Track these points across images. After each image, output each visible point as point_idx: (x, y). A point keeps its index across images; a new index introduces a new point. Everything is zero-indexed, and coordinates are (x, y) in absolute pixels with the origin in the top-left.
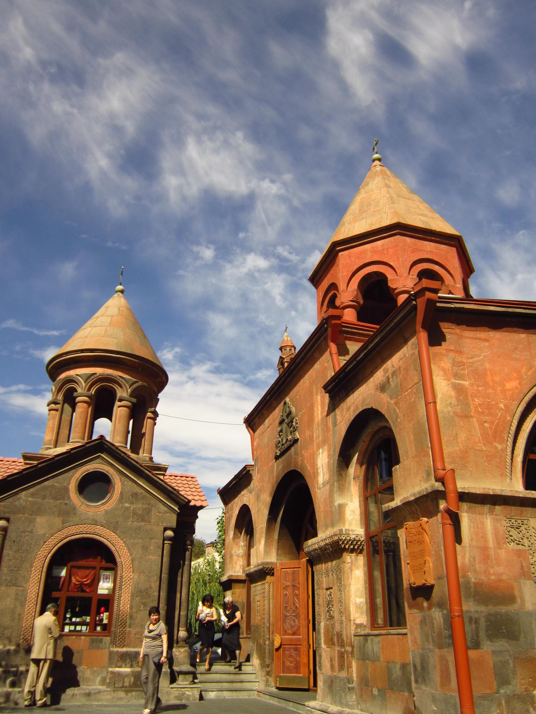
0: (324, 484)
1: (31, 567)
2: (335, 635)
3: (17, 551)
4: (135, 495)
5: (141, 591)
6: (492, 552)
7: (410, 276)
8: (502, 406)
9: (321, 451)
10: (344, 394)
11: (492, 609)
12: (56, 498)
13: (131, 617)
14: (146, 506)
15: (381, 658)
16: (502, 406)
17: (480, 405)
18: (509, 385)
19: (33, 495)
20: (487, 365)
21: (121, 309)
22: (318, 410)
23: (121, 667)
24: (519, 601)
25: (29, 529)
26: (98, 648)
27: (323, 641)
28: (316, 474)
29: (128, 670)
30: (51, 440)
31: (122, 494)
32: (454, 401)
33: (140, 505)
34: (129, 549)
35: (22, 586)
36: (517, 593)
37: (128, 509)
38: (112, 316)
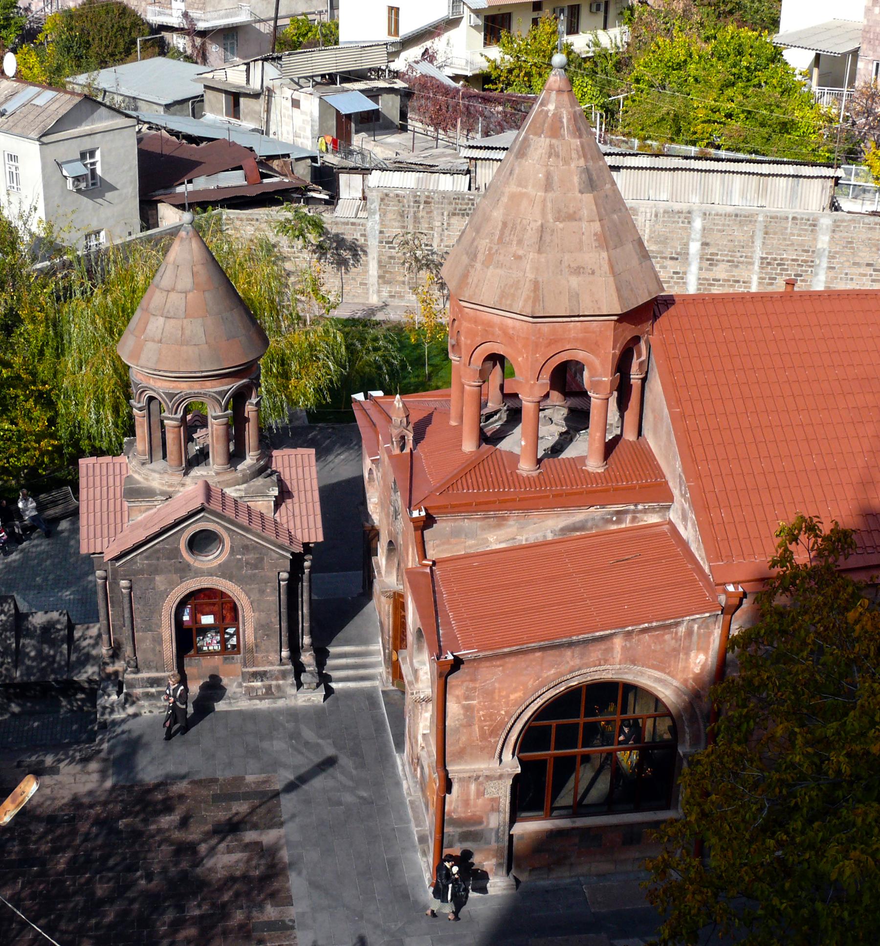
1: (161, 616)
5: (263, 626)
6: (472, 802)
7: (540, 381)
8: (503, 712)
11: (465, 829)
12: (169, 559)
13: (257, 646)
16: (503, 712)
17: (483, 715)
18: (512, 697)
19: (147, 558)
20: (497, 685)
21: (195, 269)
24: (485, 824)
25: (151, 587)
26: (232, 663)
29: (259, 684)
30: (144, 451)
31: (232, 547)
32: (462, 717)
34: (247, 595)
36: (484, 820)
37: (239, 559)
38: (186, 292)
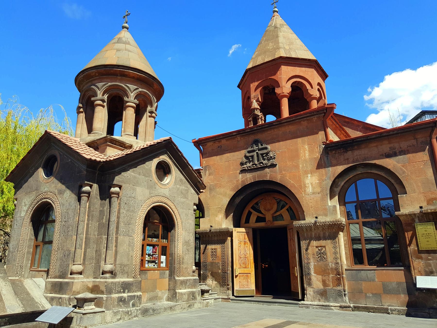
0: (313, 193)
2: (329, 269)
3: (128, 210)
4: (181, 180)
5: (186, 242)
9: (309, 175)
10: (342, 151)
14: (186, 188)
15: (376, 280)
22: (305, 153)
23: (181, 289)
27: (312, 272)
28: (303, 187)
33: (184, 188)
35: (132, 236)
37: (178, 189)
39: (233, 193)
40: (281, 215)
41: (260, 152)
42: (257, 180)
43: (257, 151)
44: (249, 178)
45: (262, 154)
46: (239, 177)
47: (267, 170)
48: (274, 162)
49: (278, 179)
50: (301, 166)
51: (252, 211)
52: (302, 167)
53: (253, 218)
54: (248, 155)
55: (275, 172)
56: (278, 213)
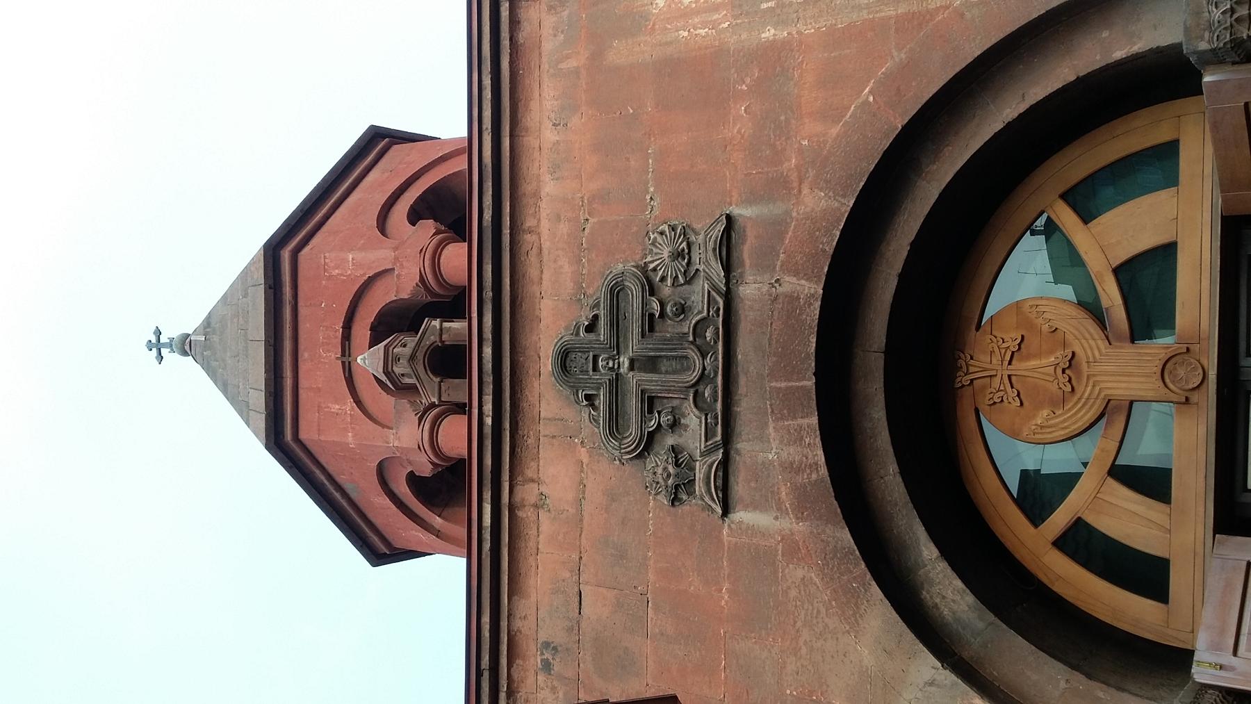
39: (878, 613)
40: (1126, 272)
41: (634, 345)
42: (810, 383)
43: (625, 361)
44: (781, 444)
45: (650, 324)
46: (764, 534)
47: (750, 290)
48: (707, 235)
49: (823, 206)
50: (769, 34)
51: (1059, 519)
52: (780, 23)
53: (1128, 519)
54: (633, 431)
55: (777, 228)
56: (1111, 295)
